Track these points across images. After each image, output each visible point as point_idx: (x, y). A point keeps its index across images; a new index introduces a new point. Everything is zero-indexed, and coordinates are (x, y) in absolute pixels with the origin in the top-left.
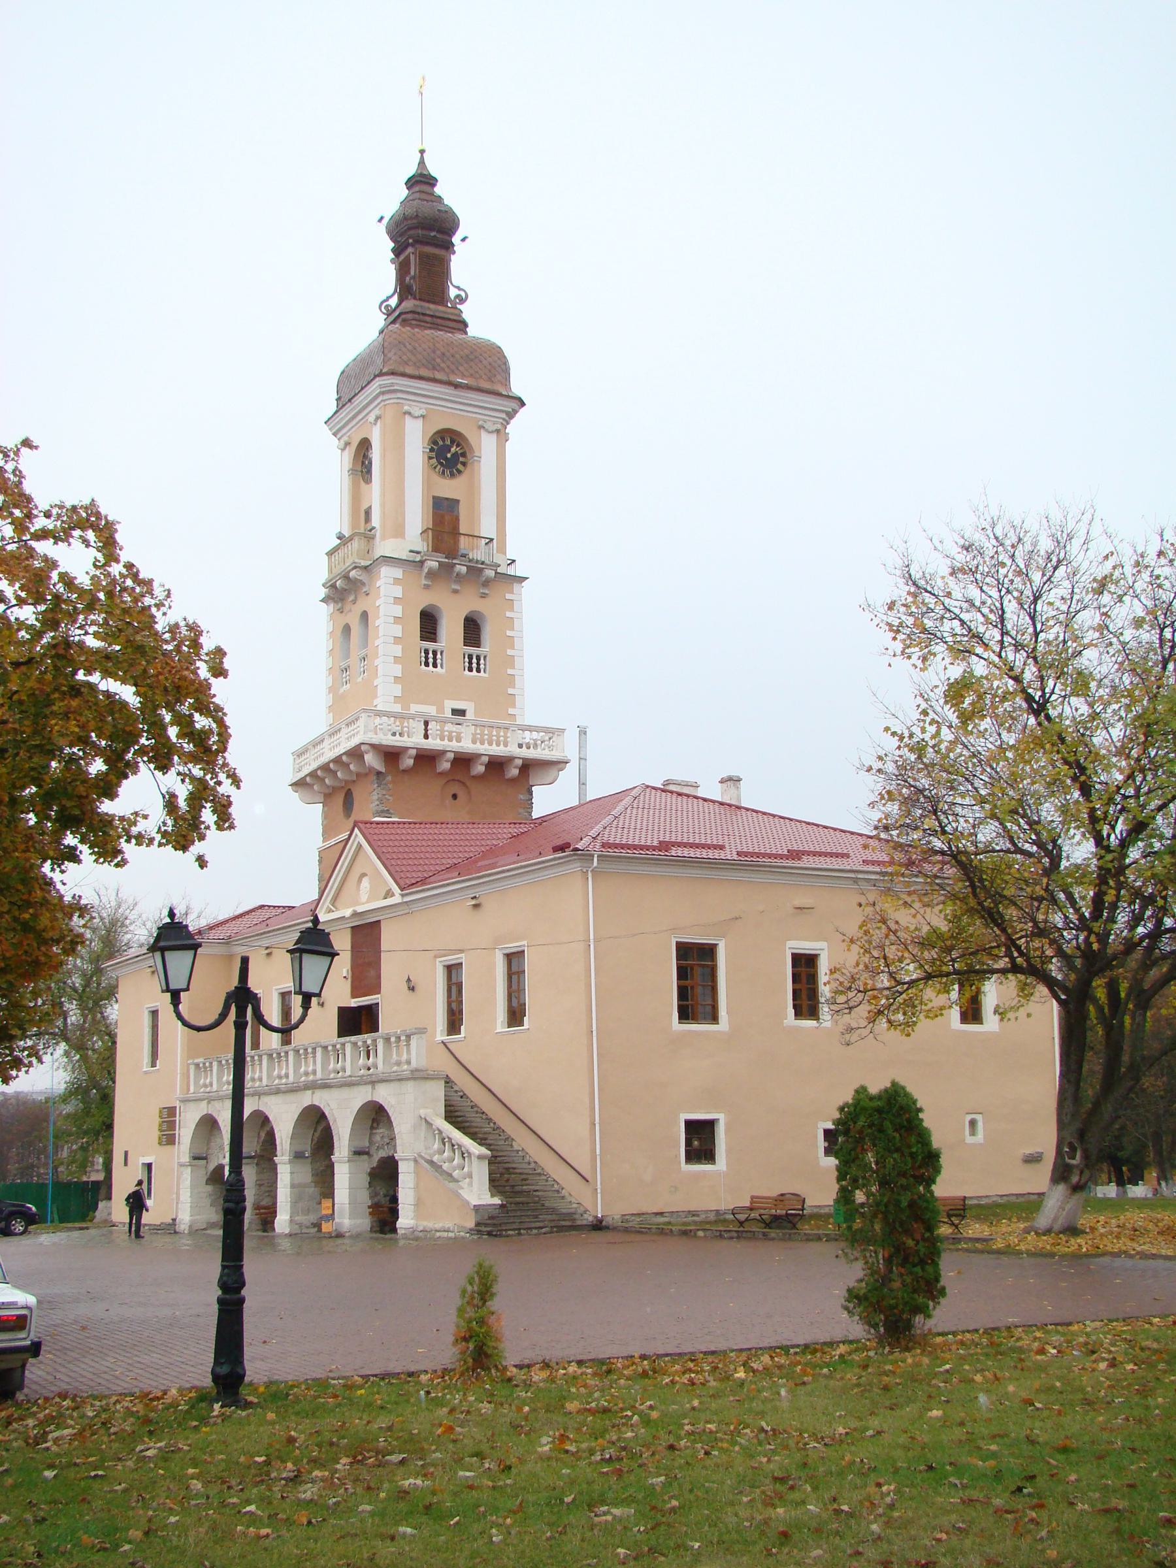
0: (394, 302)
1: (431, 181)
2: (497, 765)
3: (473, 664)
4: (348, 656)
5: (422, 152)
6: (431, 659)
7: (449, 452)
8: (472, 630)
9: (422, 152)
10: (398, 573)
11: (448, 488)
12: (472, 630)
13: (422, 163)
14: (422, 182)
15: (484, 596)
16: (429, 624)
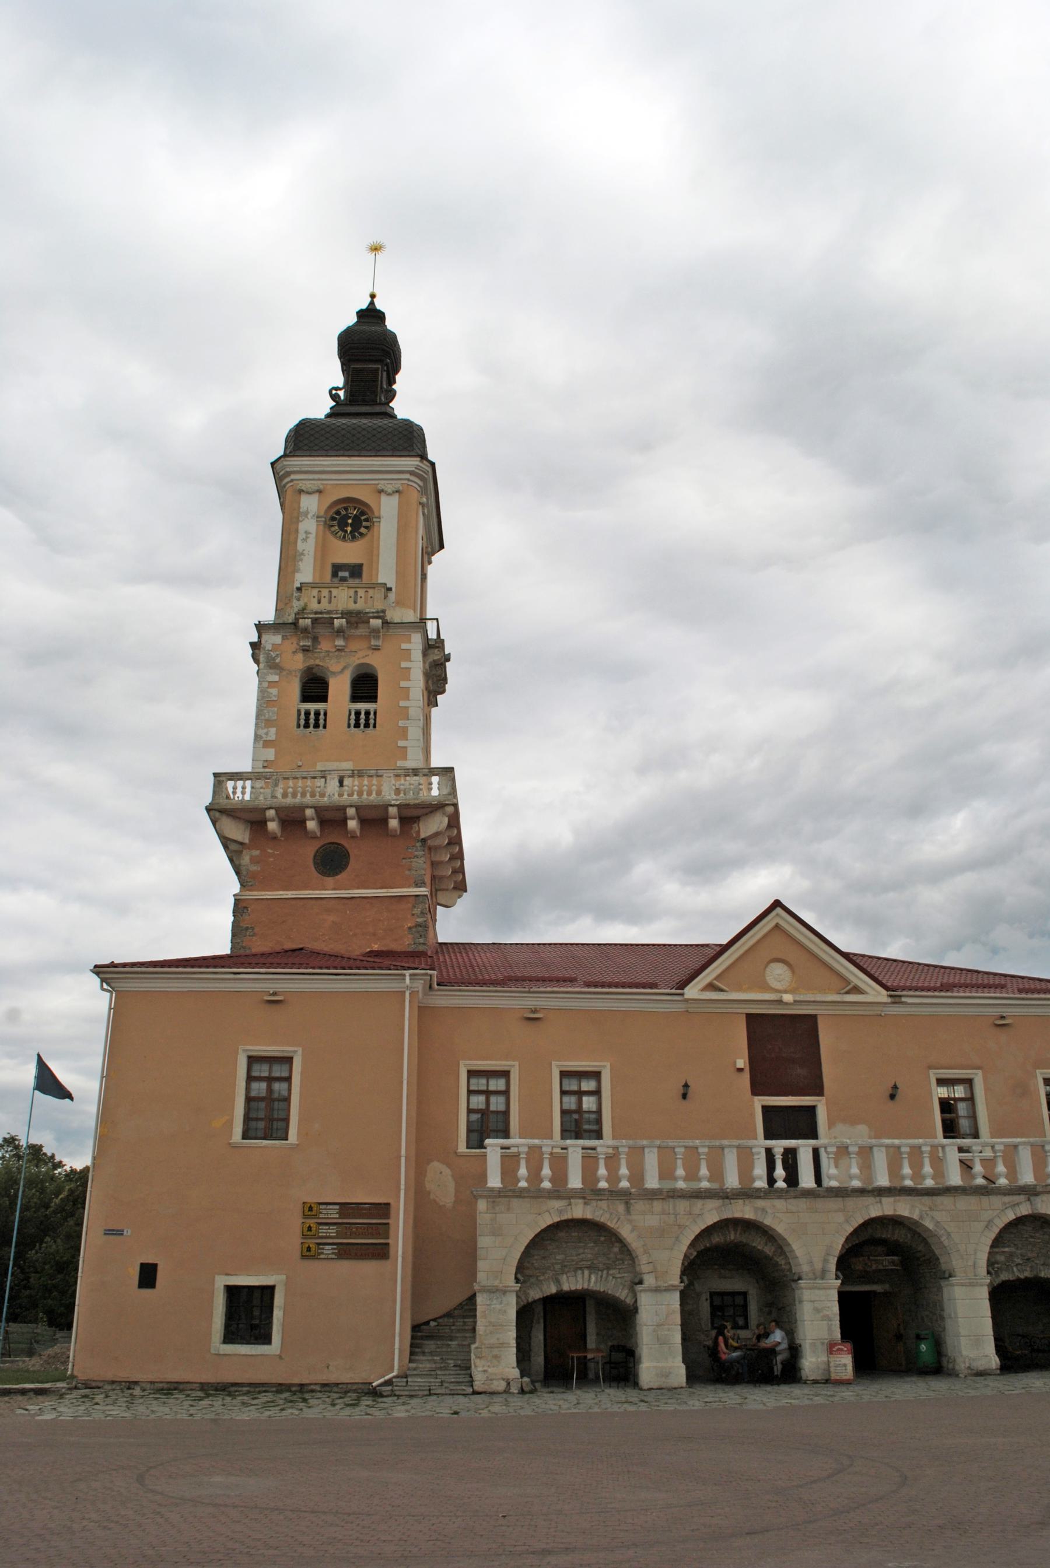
1: (380, 316)
2: (373, 819)
3: (363, 722)
5: (373, 296)
6: (314, 722)
7: (350, 519)
8: (365, 686)
9: (373, 296)
10: (277, 639)
11: (348, 552)
12: (365, 686)
13: (372, 303)
14: (371, 315)
15: (377, 649)
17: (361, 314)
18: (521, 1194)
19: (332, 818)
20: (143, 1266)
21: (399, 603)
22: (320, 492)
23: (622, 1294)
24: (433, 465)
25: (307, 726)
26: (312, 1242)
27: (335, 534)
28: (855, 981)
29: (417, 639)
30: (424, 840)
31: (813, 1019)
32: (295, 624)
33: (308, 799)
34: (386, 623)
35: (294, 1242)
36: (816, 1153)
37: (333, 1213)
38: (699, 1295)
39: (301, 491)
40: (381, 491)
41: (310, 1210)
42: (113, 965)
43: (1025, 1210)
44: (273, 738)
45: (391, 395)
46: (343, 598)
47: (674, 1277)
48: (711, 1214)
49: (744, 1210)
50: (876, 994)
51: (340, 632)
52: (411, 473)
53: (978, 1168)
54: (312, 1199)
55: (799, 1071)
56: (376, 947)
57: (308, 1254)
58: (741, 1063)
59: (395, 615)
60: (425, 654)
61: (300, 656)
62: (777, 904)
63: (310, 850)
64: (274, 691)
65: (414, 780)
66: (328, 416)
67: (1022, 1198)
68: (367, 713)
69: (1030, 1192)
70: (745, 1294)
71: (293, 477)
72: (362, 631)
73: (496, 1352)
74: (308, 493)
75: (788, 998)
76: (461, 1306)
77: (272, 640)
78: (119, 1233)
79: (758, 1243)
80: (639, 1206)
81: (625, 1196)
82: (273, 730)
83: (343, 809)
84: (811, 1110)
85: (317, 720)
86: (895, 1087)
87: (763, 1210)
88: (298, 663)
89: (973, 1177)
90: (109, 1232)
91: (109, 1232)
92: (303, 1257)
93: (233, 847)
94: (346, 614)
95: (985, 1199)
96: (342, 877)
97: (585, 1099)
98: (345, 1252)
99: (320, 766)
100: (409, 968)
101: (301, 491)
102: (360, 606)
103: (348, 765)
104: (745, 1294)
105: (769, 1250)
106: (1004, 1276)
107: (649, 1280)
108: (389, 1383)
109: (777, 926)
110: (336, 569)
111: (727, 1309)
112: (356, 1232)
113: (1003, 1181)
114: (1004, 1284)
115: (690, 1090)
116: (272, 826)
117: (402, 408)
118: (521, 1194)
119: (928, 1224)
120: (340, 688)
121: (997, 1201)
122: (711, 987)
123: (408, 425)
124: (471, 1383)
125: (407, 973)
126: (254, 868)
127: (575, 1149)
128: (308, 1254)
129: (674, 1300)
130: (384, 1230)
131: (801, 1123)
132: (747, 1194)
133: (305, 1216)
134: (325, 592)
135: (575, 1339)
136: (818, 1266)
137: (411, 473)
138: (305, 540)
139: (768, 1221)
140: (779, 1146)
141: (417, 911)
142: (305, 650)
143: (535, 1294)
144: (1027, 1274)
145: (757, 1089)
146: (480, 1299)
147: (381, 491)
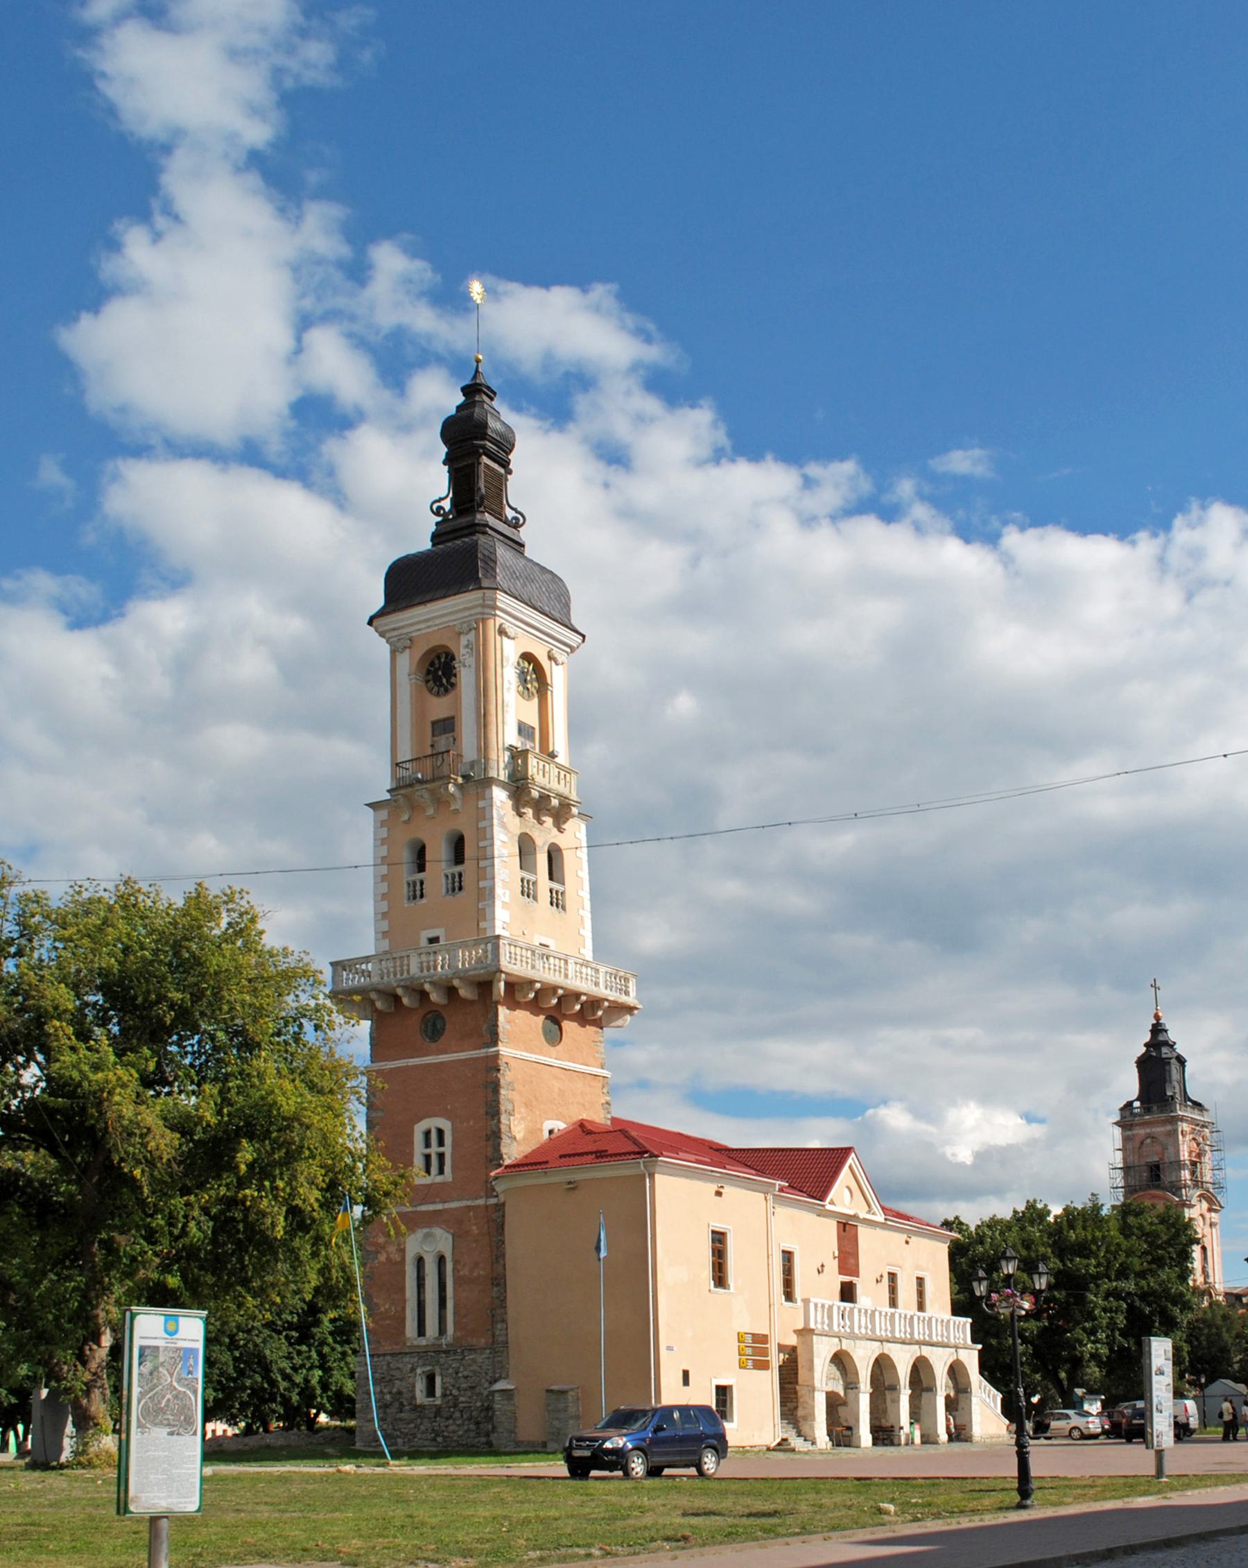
0: (447, 504)
4: (421, 868)
23: (842, 1393)
37: (749, 1339)
39: (502, 632)
44: (507, 900)
61: (518, 818)
69: (956, 1347)
71: (498, 612)
74: (509, 637)
101: (502, 632)
115: (825, 1269)
124: (814, 1443)
126: (508, 1027)
129: (868, 1396)
134: (541, 763)
138: (509, 689)
145: (843, 1270)
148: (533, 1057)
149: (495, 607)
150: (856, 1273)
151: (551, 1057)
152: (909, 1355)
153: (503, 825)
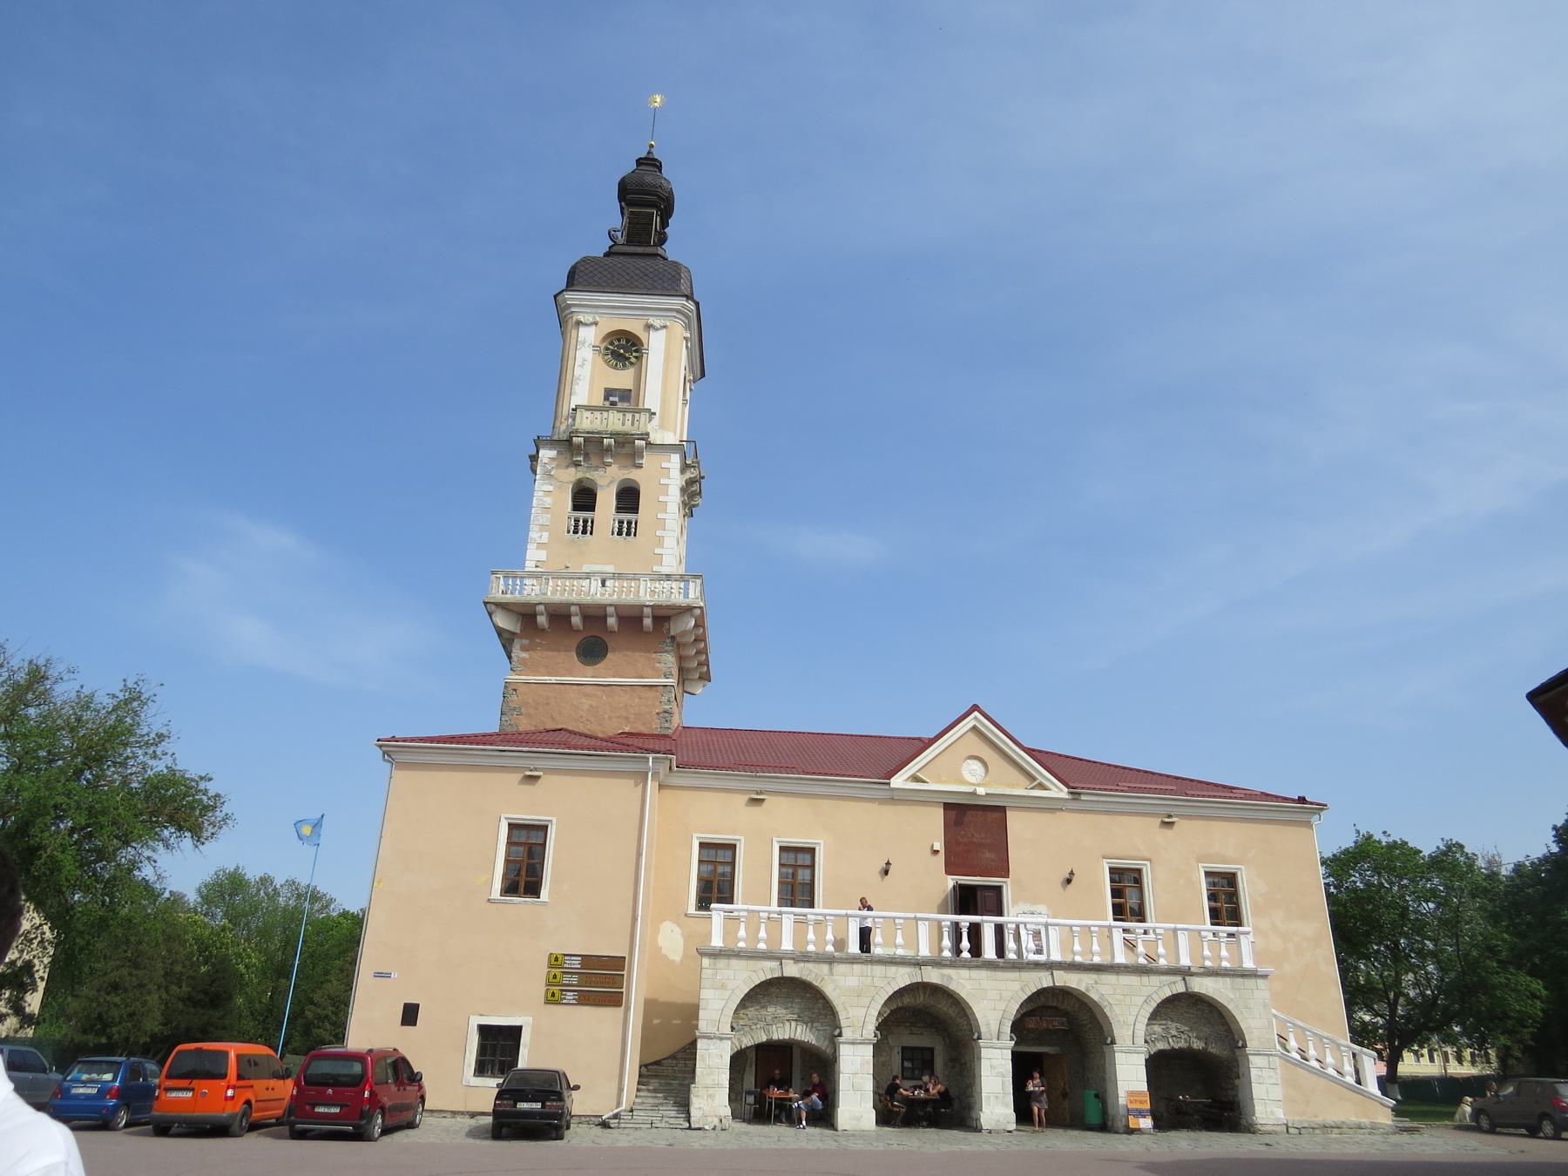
2: (631, 618)
6: (585, 528)
8: (629, 498)
10: (553, 453)
15: (640, 466)
16: (584, 498)
17: (639, 162)
18: (737, 954)
19: (594, 615)
20: (407, 1006)
21: (662, 426)
22: (596, 324)
24: (697, 304)
25: (576, 532)
26: (556, 989)
27: (607, 362)
28: (1040, 779)
29: (675, 460)
30: (673, 638)
31: (1003, 809)
32: (569, 441)
33: (574, 598)
34: (649, 444)
35: (540, 990)
36: (999, 930)
37: (576, 963)
38: (891, 1048)
40: (649, 327)
41: (555, 961)
42: (394, 739)
43: (1180, 988)
44: (545, 539)
45: (662, 239)
46: (615, 421)
47: (870, 1030)
48: (903, 977)
49: (933, 976)
50: (1058, 791)
51: (609, 449)
52: (678, 311)
53: (1141, 949)
54: (558, 951)
55: (988, 855)
56: (627, 729)
57: (552, 999)
58: (939, 846)
59: (656, 438)
60: (683, 471)
61: (572, 470)
62: (975, 708)
63: (574, 642)
64: (548, 501)
65: (666, 584)
66: (607, 255)
67: (1178, 978)
68: (629, 523)
69: (1185, 973)
70: (931, 1050)
72: (627, 450)
73: (711, 1091)
75: (981, 791)
76: (684, 1050)
77: (546, 454)
78: (387, 975)
79: (943, 1007)
80: (840, 968)
81: (830, 960)
82: (545, 535)
83: (604, 607)
84: (998, 890)
85: (585, 527)
86: (1072, 873)
87: (950, 978)
88: (571, 475)
89: (1138, 956)
90: (379, 975)
91: (379, 975)
92: (547, 1002)
93: (505, 635)
94: (613, 435)
95: (1145, 979)
96: (601, 665)
97: (800, 872)
98: (585, 999)
99: (586, 568)
100: (648, 751)
101: (579, 323)
102: (628, 428)
103: (610, 569)
104: (931, 1050)
105: (952, 1012)
106: (1161, 1046)
107: (847, 1034)
108: (616, 1116)
109: (974, 728)
110: (609, 393)
111: (918, 1061)
112: (597, 980)
113: (1162, 962)
114: (1161, 1053)
116: (542, 620)
117: (672, 250)
118: (737, 954)
119: (1094, 996)
120: (606, 500)
121: (1155, 980)
122: (915, 779)
123: (676, 265)
125: (651, 756)
126: (525, 655)
127: (789, 915)
128: (552, 999)
130: (617, 981)
131: (991, 901)
132: (937, 963)
133: (551, 966)
134: (598, 414)
135: (783, 1081)
136: (994, 1028)
137: (678, 311)
139: (952, 987)
140: (965, 920)
141: (664, 699)
142: (577, 464)
143: (747, 1042)
144: (1182, 1044)
145: (950, 869)
146: (700, 1044)
147: (649, 327)
148: (553, 679)
149: (570, 306)
150: (1005, 873)
151: (587, 676)
152: (1016, 986)
153: (548, 474)
